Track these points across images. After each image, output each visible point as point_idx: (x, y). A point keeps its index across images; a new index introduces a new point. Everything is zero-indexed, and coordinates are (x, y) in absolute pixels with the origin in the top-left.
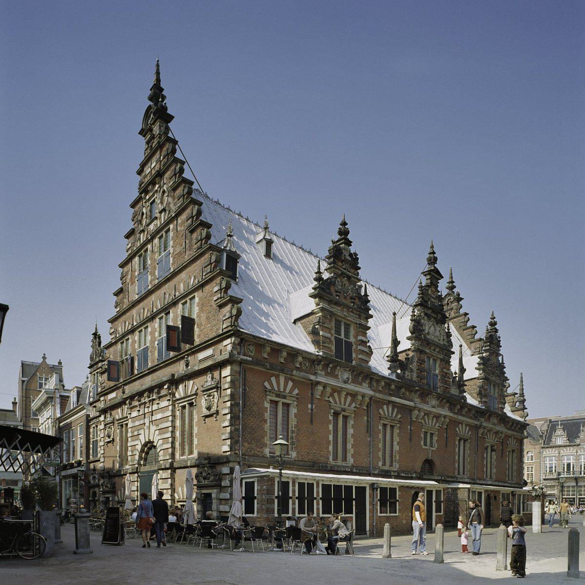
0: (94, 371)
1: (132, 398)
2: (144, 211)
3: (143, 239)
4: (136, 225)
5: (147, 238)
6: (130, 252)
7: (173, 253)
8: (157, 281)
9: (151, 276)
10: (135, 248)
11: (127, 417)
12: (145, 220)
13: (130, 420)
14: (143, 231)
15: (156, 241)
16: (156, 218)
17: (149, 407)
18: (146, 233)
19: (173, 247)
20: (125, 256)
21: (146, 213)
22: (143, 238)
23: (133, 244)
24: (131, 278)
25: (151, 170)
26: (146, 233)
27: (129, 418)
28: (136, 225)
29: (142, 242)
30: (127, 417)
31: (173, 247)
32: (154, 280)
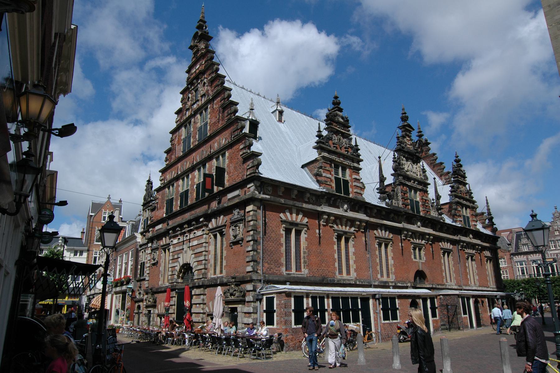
0: (146, 208)
1: (174, 229)
2: (190, 95)
3: (188, 114)
4: (184, 105)
5: (191, 114)
6: (178, 123)
7: (210, 123)
8: (197, 143)
9: (193, 139)
10: (182, 121)
11: (169, 244)
12: (190, 102)
13: (172, 246)
14: (188, 109)
15: (198, 116)
16: (198, 101)
17: (187, 236)
18: (190, 110)
19: (210, 119)
20: (174, 126)
21: (191, 97)
22: (188, 114)
23: (181, 118)
24: (178, 141)
25: (196, 70)
26: (190, 110)
27: (171, 244)
28: (184, 105)
29: (187, 116)
30: (169, 244)
31: (210, 119)
32: (195, 141)
